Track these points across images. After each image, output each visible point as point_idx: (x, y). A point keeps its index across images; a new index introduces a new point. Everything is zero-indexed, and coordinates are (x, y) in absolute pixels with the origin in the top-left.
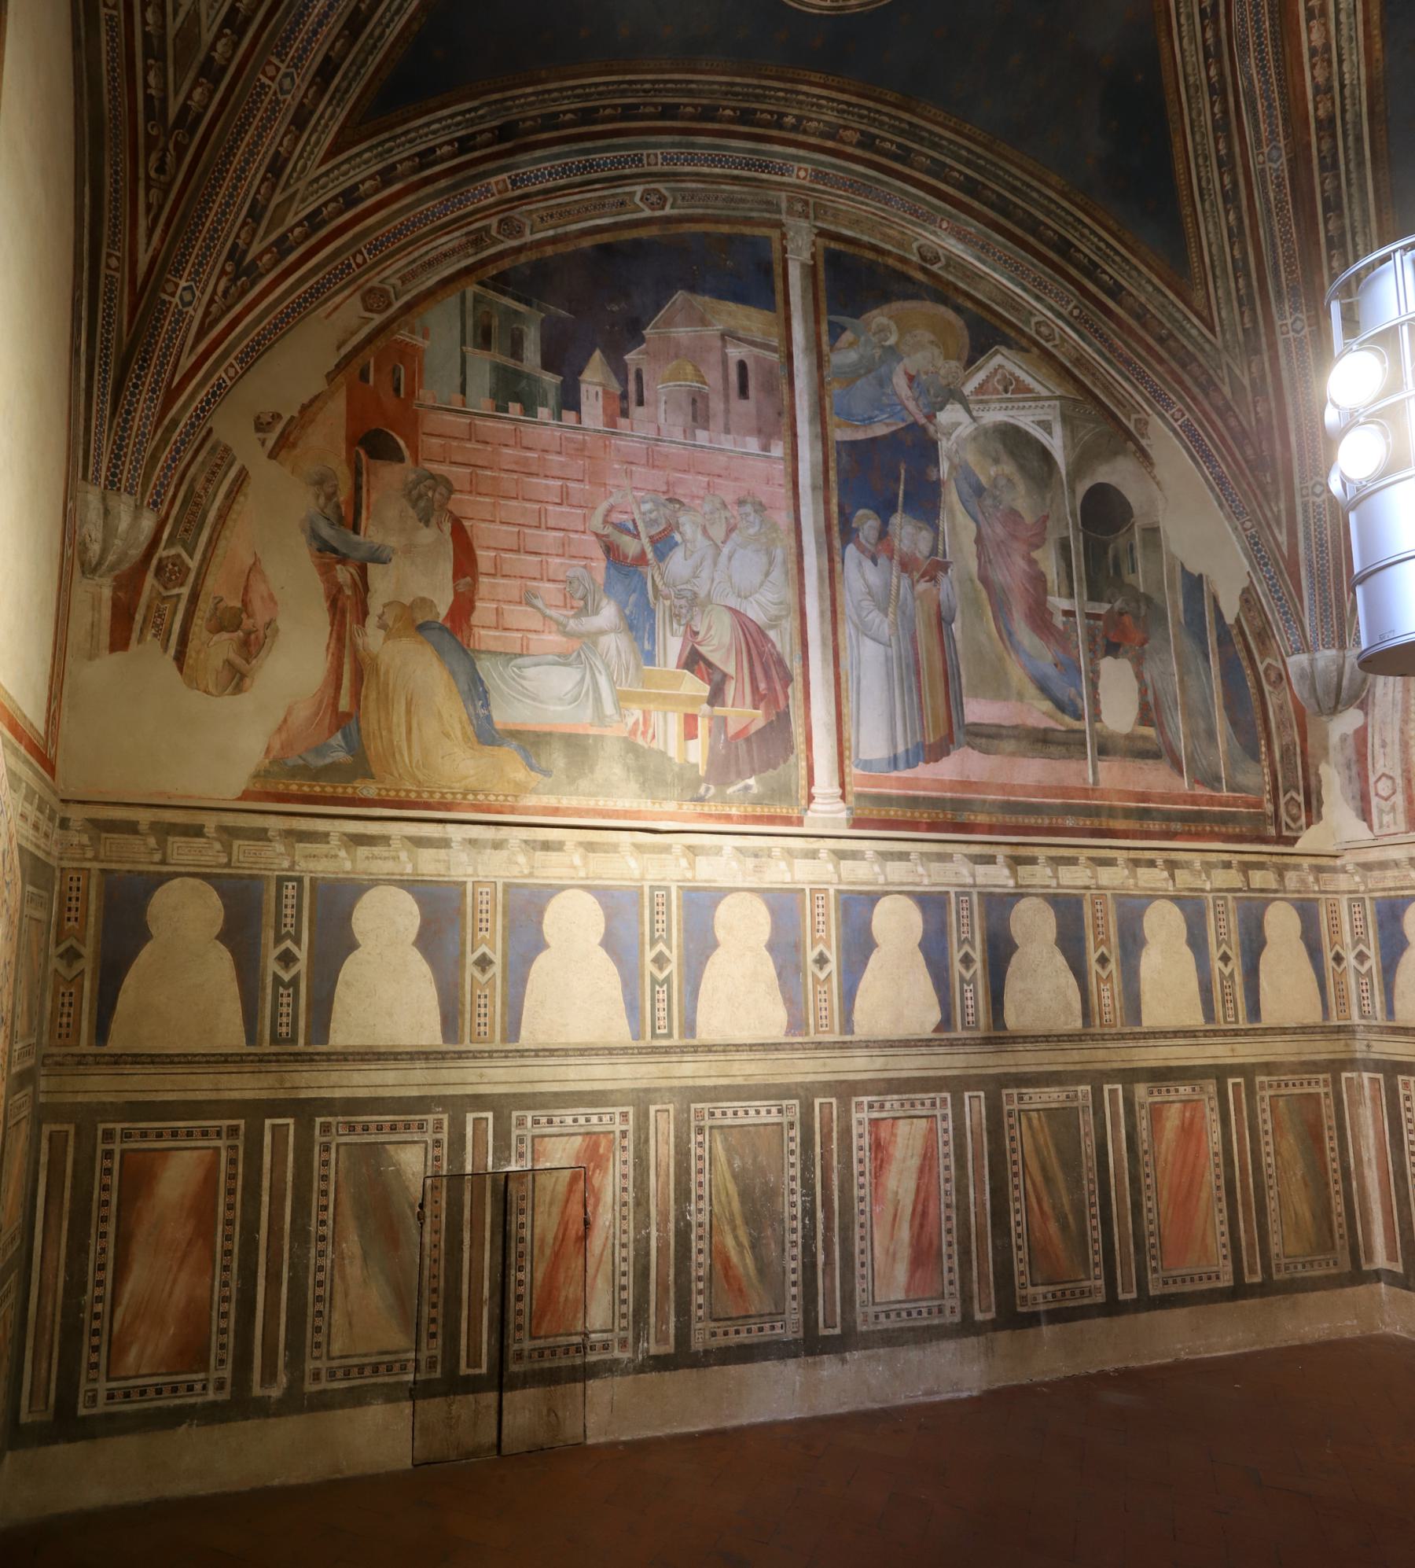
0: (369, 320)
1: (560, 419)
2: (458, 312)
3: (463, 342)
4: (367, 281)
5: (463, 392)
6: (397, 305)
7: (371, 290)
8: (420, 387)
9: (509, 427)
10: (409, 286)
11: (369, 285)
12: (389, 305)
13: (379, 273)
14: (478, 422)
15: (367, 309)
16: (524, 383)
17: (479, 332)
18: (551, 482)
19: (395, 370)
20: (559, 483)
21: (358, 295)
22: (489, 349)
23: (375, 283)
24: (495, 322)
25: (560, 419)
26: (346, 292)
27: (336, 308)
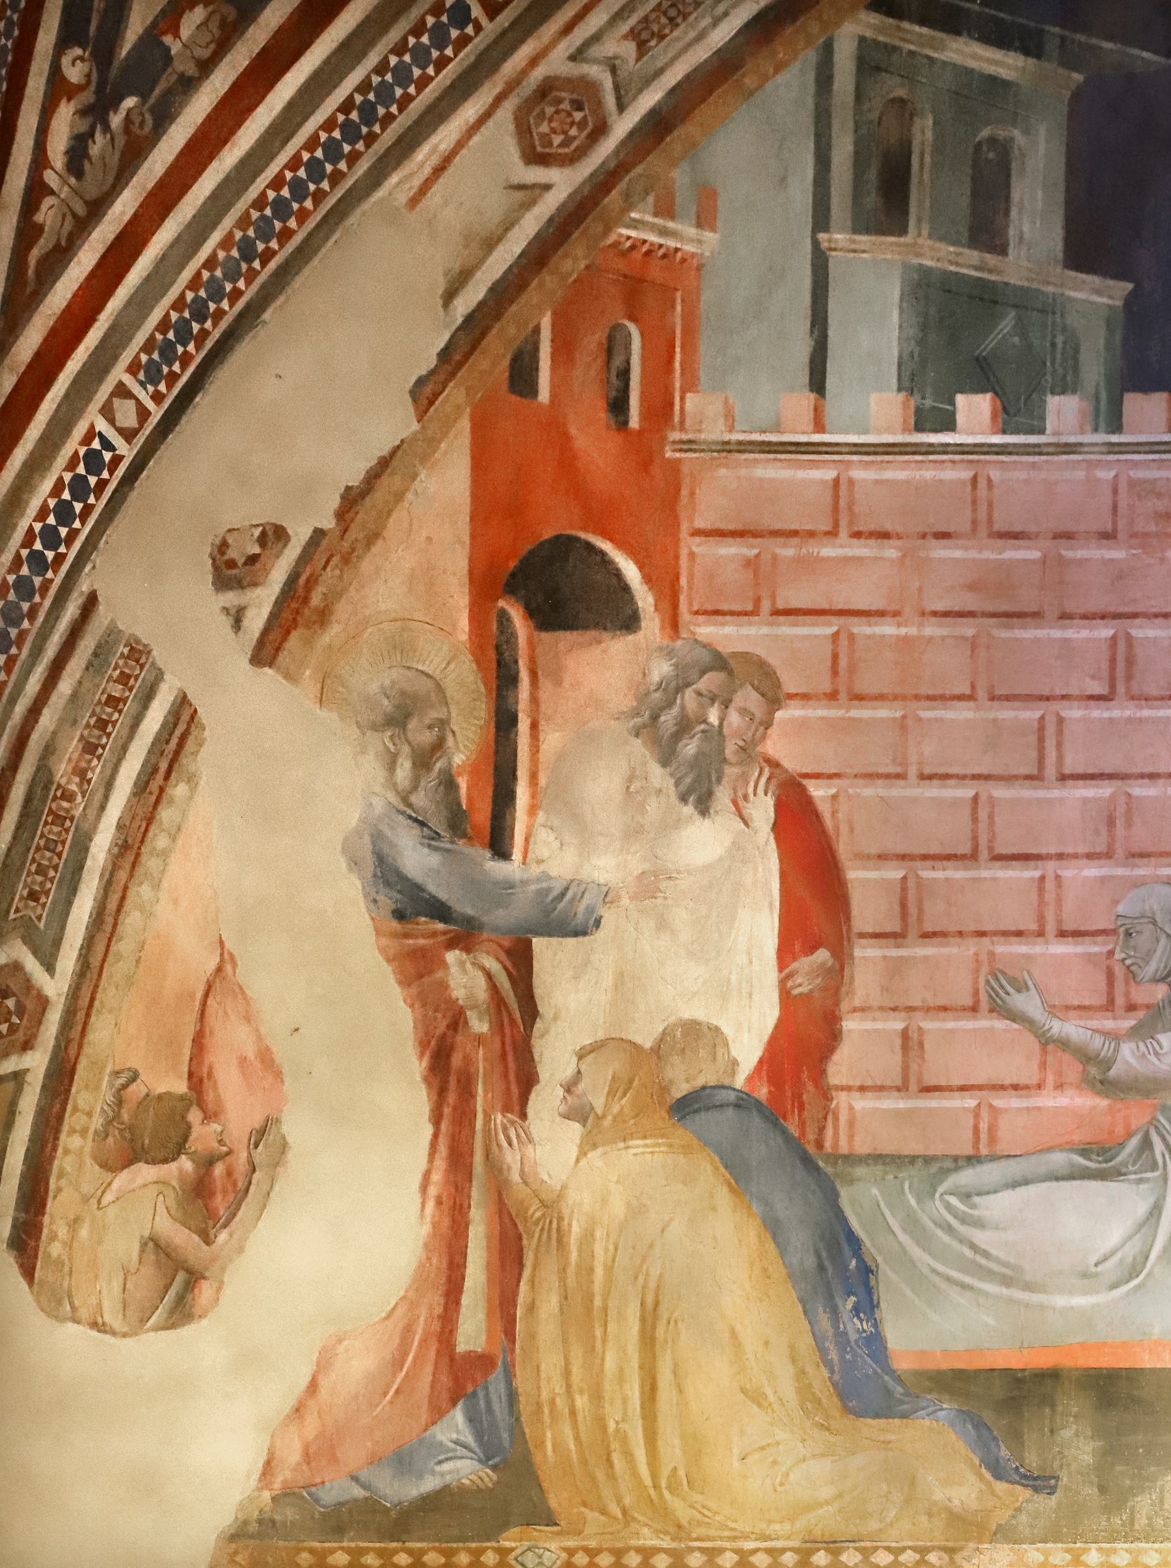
0: (535, 191)
1: (1116, 426)
2: (806, 118)
3: (821, 220)
4: (534, 62)
5: (818, 383)
6: (623, 126)
7: (545, 90)
8: (690, 385)
9: (956, 473)
10: (659, 53)
11: (539, 73)
12: (601, 130)
13: (568, 29)
14: (862, 473)
15: (535, 157)
16: (1007, 323)
17: (872, 175)
18: (1079, 633)
19: (614, 344)
20: (1105, 632)
21: (505, 114)
22: (902, 231)
23: (557, 63)
24: (924, 131)
25: (1116, 426)
26: (469, 111)
27: (439, 170)
